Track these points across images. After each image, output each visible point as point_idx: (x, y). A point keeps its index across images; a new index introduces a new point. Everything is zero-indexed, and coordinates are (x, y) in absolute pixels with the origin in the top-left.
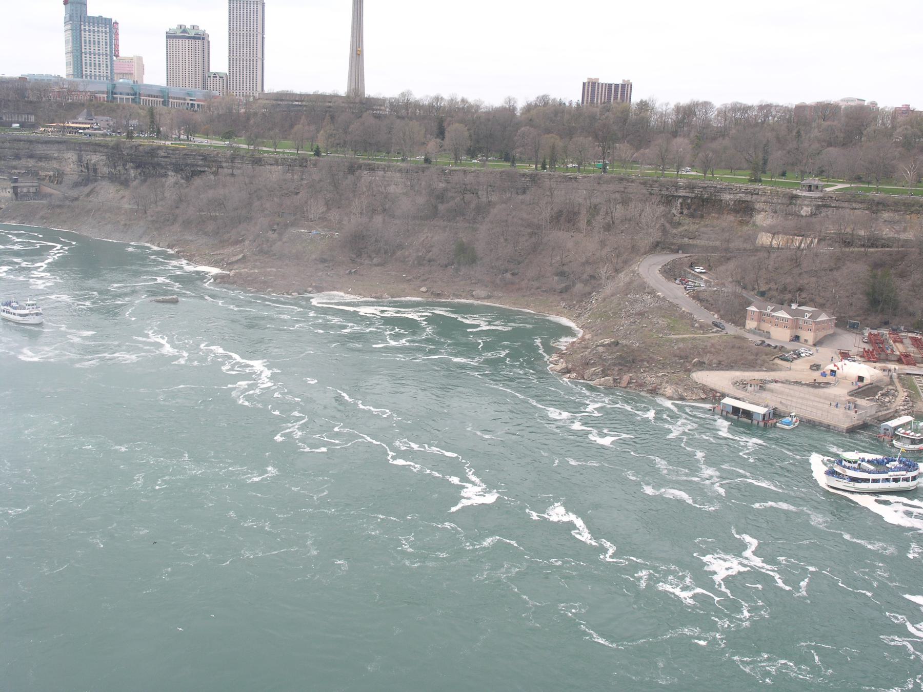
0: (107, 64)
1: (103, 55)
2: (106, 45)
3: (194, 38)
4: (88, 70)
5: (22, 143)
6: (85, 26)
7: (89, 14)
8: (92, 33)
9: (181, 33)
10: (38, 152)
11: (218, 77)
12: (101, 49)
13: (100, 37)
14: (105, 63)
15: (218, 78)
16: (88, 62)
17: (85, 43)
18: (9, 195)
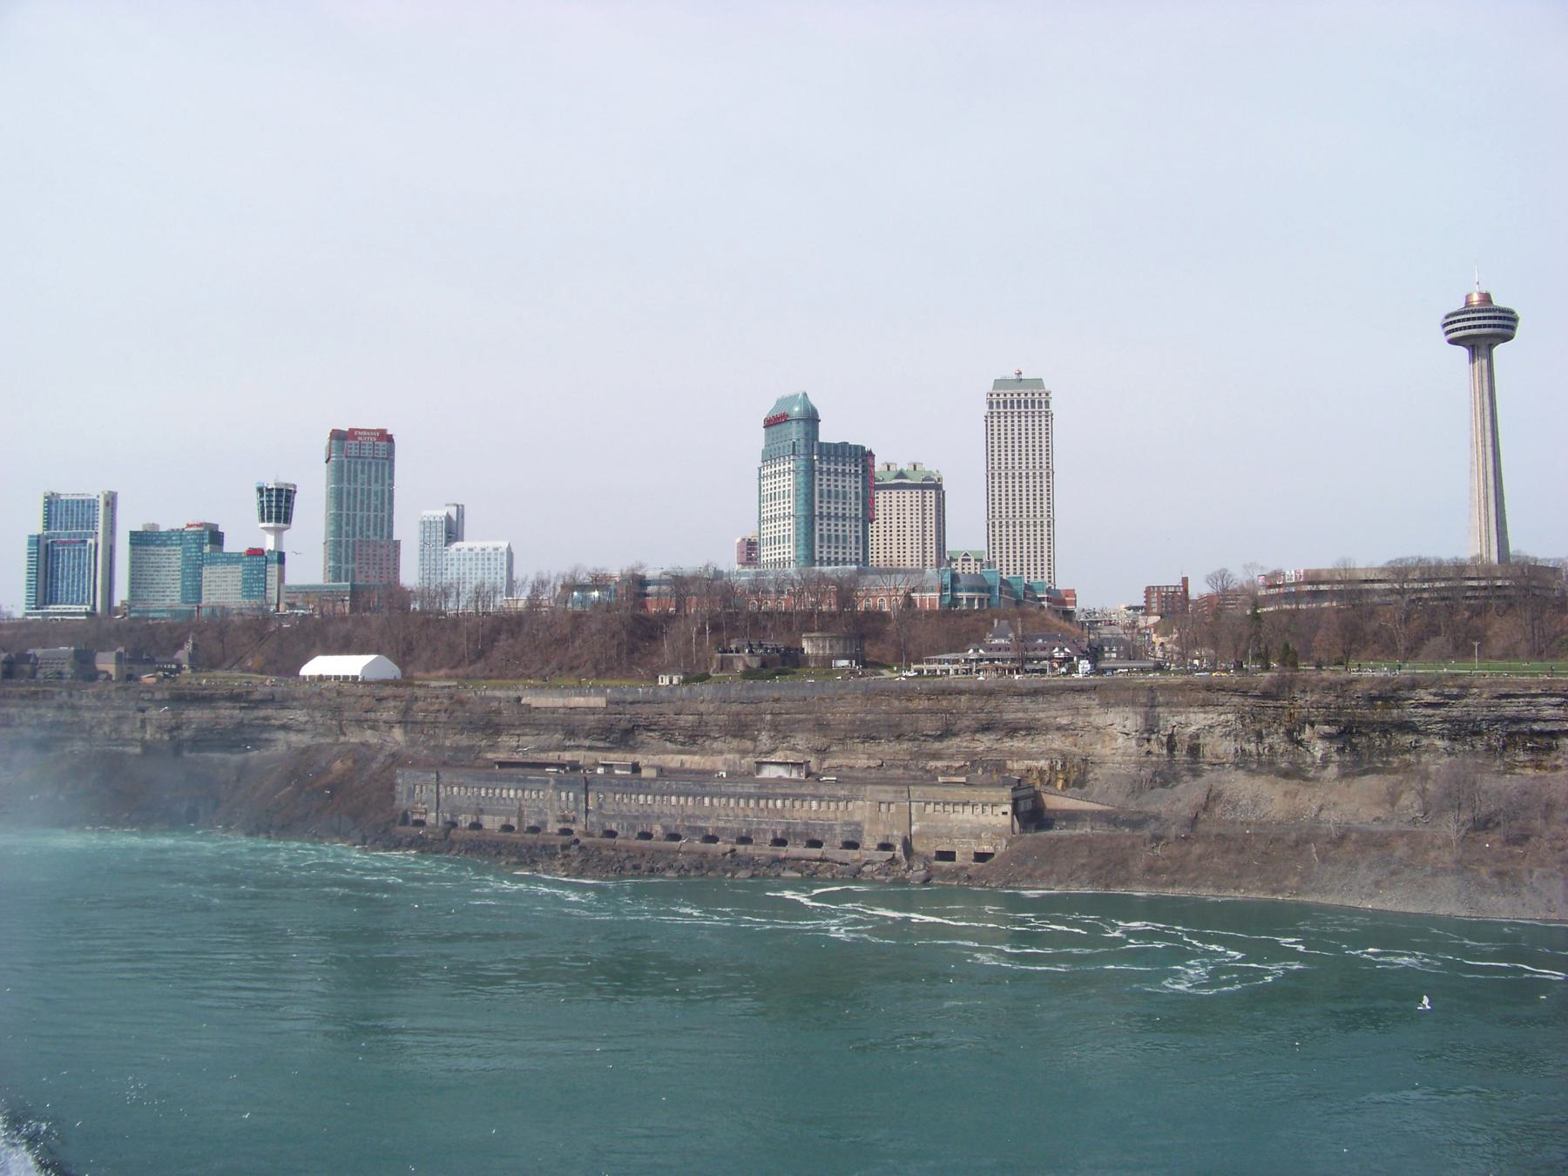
0: (857, 537)
1: (850, 518)
2: (857, 499)
3: (922, 487)
4: (825, 550)
5: (963, 698)
6: (821, 463)
7: (821, 440)
8: (832, 477)
9: (897, 477)
10: (1006, 716)
11: (973, 560)
12: (847, 506)
13: (847, 484)
14: (853, 534)
15: (972, 562)
16: (825, 533)
17: (821, 496)
18: (1007, 820)
